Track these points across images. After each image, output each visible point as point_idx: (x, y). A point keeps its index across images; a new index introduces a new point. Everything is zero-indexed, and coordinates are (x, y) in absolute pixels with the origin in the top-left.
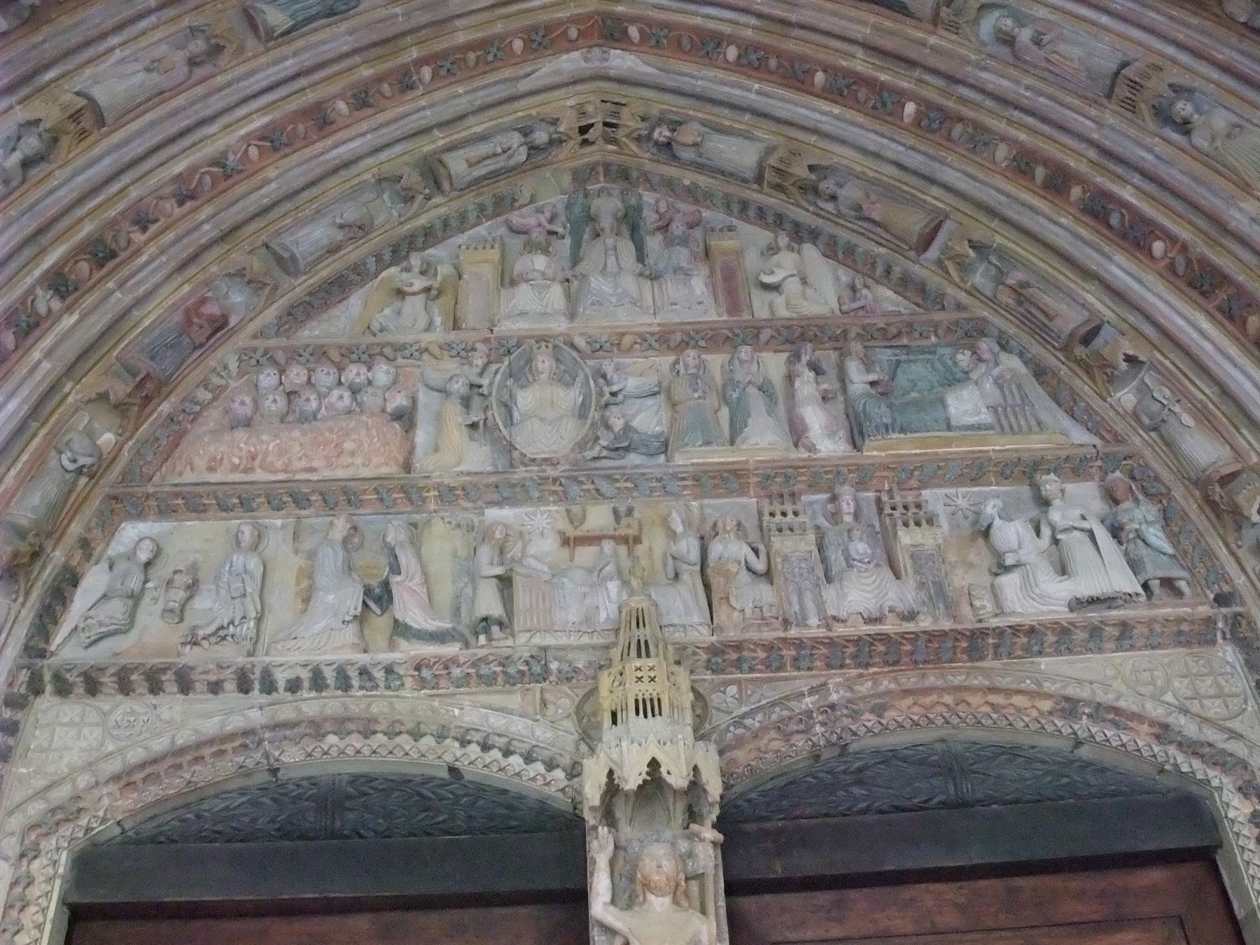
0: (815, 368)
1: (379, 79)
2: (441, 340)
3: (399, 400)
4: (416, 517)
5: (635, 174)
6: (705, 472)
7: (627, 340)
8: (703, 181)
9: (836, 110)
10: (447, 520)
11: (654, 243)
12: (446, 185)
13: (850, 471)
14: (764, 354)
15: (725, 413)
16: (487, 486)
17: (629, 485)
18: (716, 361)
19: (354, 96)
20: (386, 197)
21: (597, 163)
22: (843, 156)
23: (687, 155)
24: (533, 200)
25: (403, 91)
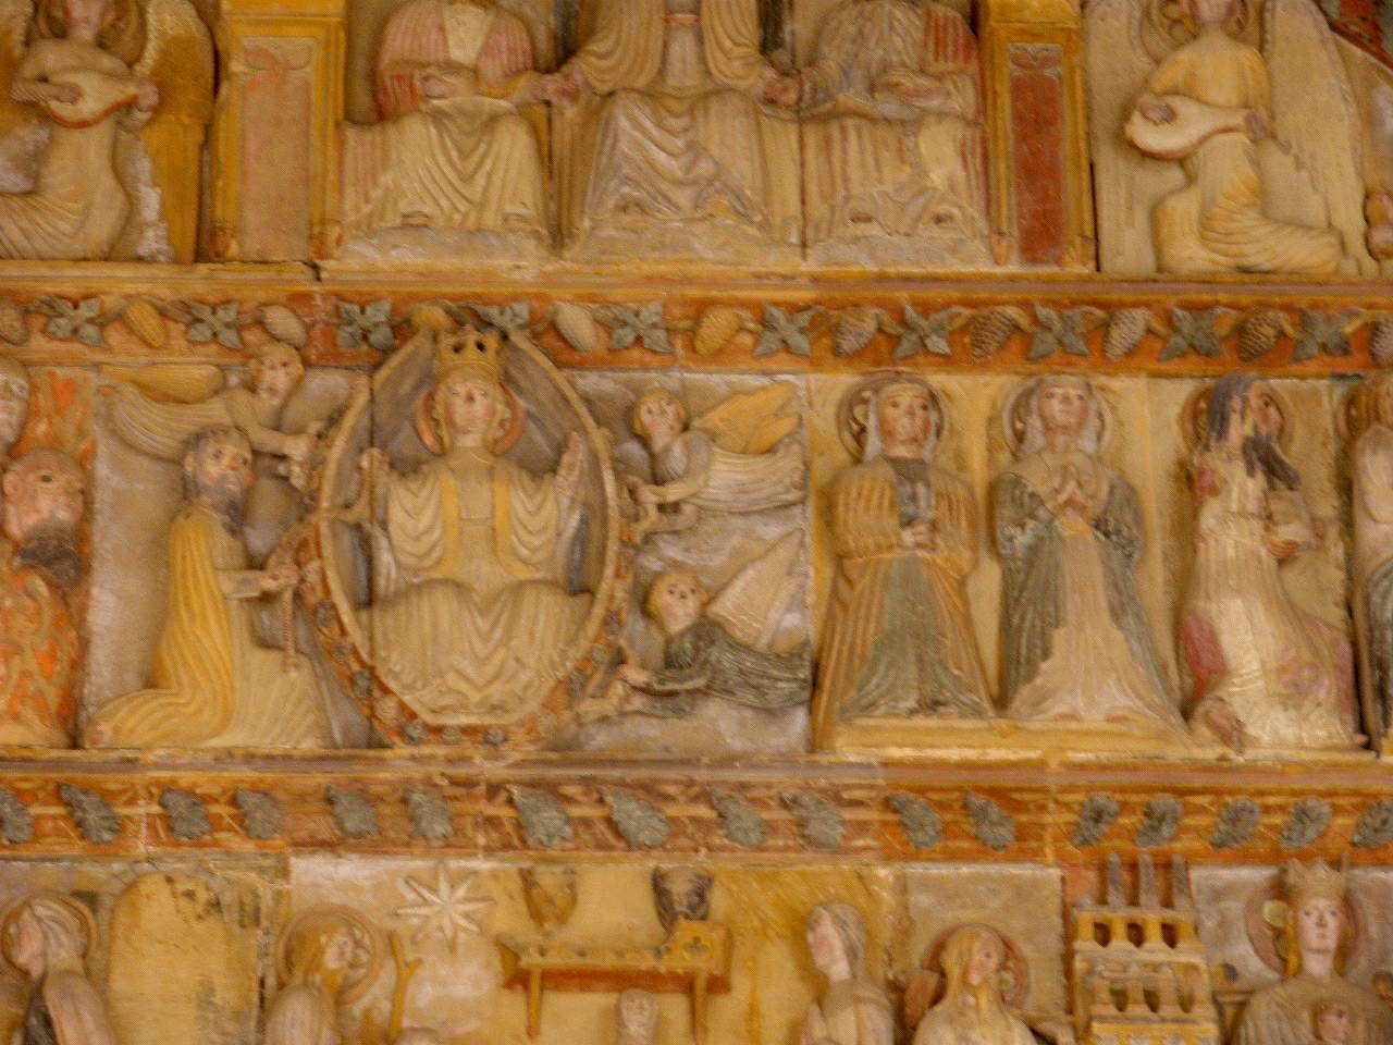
0: (1268, 462)
2: (166, 294)
4: (95, 873)
6: (921, 791)
7: (717, 324)
10: (181, 887)
13: (1337, 810)
14: (1116, 384)
15: (987, 582)
16: (301, 798)
17: (703, 811)
18: (977, 395)
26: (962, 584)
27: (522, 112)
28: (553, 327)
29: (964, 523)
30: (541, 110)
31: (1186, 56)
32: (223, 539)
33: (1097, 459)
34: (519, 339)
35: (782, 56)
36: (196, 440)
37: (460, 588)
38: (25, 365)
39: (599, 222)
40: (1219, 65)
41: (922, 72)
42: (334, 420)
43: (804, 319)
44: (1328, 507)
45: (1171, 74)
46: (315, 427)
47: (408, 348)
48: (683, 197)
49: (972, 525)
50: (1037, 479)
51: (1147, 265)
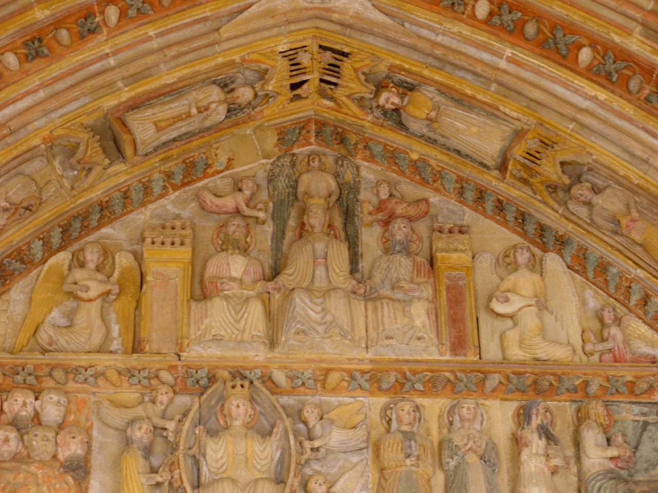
0: (546, 433)
1: (57, 23)
2: (121, 365)
3: (72, 448)
5: (353, 138)
7: (334, 378)
8: (435, 157)
9: (603, 95)
11: (370, 238)
12: (129, 151)
14: (488, 403)
15: (439, 480)
18: (434, 406)
19: (25, 44)
20: (56, 163)
21: (309, 121)
22: (604, 152)
23: (414, 126)
24: (230, 164)
25: (82, 37)
26: (429, 481)
27: (259, 296)
28: (270, 378)
29: (430, 456)
30: (266, 295)
31: (512, 277)
32: (141, 461)
33: (481, 432)
34: (257, 383)
35: (358, 276)
36: (132, 422)
37: (234, 481)
38: (66, 393)
39: (288, 339)
40: (525, 281)
41: (412, 282)
42: (185, 415)
43: (367, 376)
44: (570, 452)
45: (507, 284)
46: (178, 417)
47: (215, 386)
48: (321, 329)
49: (433, 457)
50: (458, 440)
51: (498, 356)
